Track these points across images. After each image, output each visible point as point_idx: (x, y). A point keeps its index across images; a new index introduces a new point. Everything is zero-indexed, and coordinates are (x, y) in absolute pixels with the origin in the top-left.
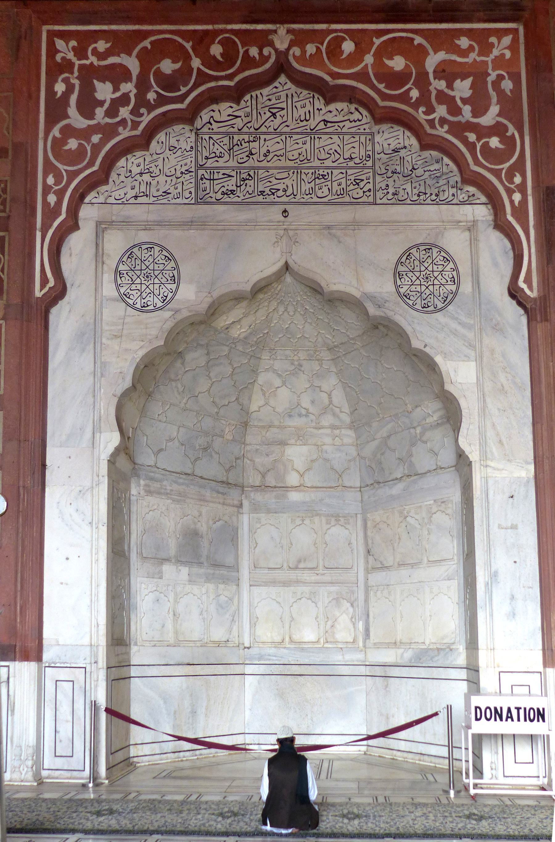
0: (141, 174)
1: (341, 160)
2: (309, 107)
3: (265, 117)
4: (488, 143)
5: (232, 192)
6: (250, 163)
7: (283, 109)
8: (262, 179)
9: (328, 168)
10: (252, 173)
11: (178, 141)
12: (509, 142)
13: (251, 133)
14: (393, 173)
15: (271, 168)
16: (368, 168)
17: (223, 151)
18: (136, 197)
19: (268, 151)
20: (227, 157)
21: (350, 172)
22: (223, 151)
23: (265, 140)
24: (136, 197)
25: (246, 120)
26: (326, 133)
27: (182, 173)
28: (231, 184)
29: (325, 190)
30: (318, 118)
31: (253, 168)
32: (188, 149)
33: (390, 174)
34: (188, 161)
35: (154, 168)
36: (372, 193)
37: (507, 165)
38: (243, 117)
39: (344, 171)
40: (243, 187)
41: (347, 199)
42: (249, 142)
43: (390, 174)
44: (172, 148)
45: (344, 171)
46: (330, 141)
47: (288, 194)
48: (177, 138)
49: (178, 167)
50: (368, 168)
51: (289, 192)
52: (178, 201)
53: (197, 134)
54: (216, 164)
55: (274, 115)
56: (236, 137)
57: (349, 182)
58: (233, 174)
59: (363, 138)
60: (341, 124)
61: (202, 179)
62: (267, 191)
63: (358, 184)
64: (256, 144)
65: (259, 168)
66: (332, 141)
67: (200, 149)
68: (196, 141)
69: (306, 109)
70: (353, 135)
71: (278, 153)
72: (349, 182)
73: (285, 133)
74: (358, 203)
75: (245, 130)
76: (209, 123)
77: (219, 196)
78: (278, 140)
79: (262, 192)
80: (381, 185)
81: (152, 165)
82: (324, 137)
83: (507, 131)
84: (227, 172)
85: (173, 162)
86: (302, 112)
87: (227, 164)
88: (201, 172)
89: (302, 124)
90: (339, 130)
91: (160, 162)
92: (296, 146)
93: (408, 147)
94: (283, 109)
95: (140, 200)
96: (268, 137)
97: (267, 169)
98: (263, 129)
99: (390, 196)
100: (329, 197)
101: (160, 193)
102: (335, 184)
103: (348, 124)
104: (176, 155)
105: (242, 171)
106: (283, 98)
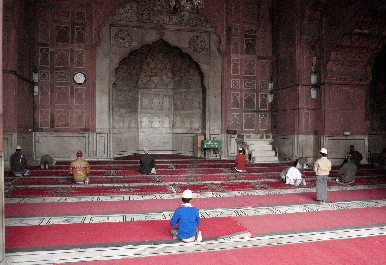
0: (122, 13)
5: (147, 20)
18: (121, 19)
23: (157, 7)
24: (121, 19)
28: (147, 17)
29: (172, 21)
32: (135, 7)
34: (135, 11)
44: (131, 7)
51: (162, 21)
53: (138, 4)
54: (143, 12)
56: (149, 6)
58: (148, 15)
64: (154, 8)
68: (138, 6)
77: (144, 20)
79: (155, 20)
84: (146, 14)
95: (122, 20)
96: (158, 6)
97: (157, 15)
98: (156, 4)
102: (175, 20)
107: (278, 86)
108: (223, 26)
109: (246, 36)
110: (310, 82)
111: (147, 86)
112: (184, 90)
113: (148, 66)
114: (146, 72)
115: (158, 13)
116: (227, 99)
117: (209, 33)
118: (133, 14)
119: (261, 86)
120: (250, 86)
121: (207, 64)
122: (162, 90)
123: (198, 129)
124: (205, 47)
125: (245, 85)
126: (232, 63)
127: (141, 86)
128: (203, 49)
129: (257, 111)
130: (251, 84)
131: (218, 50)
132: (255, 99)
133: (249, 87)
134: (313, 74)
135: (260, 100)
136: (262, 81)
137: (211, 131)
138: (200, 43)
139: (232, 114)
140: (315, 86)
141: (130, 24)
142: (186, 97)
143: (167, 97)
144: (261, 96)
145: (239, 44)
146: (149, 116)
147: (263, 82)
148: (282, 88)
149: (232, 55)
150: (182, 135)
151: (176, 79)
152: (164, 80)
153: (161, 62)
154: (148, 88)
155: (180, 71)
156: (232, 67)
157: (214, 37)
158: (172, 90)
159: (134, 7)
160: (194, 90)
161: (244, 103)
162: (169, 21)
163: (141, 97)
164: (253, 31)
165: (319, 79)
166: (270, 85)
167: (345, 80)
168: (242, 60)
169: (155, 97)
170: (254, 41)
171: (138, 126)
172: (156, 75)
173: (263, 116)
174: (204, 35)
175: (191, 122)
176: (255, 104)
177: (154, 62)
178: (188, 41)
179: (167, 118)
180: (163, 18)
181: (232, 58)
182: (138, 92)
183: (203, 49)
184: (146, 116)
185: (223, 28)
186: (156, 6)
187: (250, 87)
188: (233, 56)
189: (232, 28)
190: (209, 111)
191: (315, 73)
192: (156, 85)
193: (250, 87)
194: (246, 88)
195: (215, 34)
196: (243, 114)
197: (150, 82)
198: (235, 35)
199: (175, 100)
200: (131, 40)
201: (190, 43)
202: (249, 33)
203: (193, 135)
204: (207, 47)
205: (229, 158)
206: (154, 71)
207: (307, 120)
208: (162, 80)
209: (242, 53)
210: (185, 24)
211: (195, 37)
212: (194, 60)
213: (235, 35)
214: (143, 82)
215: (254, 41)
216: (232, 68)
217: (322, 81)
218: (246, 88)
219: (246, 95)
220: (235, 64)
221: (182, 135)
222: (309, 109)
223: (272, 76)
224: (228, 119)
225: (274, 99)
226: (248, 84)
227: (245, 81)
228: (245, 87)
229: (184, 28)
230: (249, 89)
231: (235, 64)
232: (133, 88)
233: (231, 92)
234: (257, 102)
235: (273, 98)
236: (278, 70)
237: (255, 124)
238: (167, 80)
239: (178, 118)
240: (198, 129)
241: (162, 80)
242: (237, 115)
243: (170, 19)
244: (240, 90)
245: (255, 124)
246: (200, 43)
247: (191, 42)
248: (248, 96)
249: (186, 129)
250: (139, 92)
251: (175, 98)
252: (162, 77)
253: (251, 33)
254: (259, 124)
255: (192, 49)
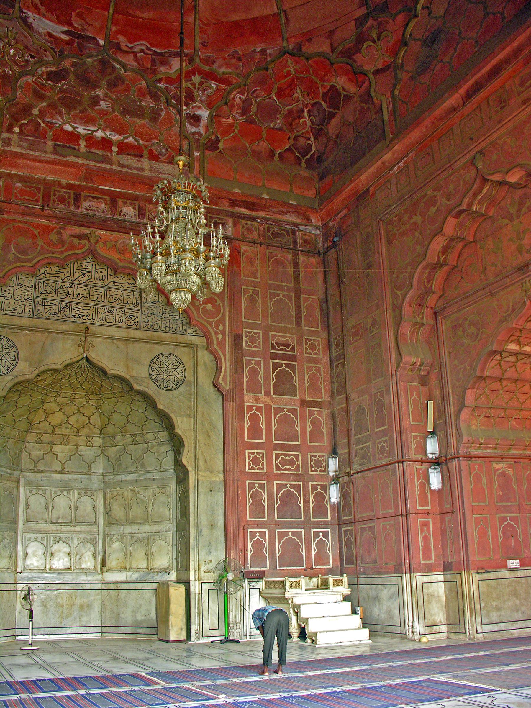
1: (122, 304)
2: (105, 273)
3: (78, 275)
4: (206, 307)
5: (56, 313)
6: (67, 299)
7: (90, 272)
8: (75, 309)
9: (115, 307)
10: (68, 305)
11: (24, 281)
12: (218, 308)
13: (69, 283)
14: (151, 314)
15: (80, 303)
16: (138, 310)
17: (51, 290)
19: (79, 294)
20: (53, 294)
21: (127, 311)
22: (51, 290)
23: (77, 287)
25: (67, 275)
26: (115, 289)
27: (25, 299)
28: (55, 309)
30: (110, 280)
31: (69, 302)
32: (30, 286)
33: (149, 315)
35: (7, 294)
36: (139, 324)
37: (215, 319)
38: (65, 273)
39: (123, 310)
40: (62, 312)
41: (124, 325)
42: (68, 287)
43: (149, 315)
44: (20, 285)
45: (123, 310)
46: (116, 293)
47: (89, 318)
48: (24, 279)
49: (23, 296)
50: (138, 310)
51: (90, 318)
52: (21, 315)
53: (36, 279)
54: (47, 297)
55: (84, 274)
56: (60, 284)
57: (126, 316)
58: (57, 303)
59: (135, 293)
60: (123, 285)
61: (37, 304)
62: (77, 315)
63: (131, 318)
64: (72, 289)
65: (73, 302)
66: (117, 293)
67: (37, 287)
68: (36, 282)
69: (103, 274)
70: (130, 291)
71: (85, 296)
72: (126, 316)
73: (91, 285)
74: (131, 328)
75: (66, 280)
76: (44, 273)
77: (47, 315)
78: (86, 288)
79: (74, 316)
80: (144, 320)
81: (7, 292)
82: (113, 290)
83: (216, 302)
84: (53, 302)
85: (21, 293)
86: (101, 275)
87: (53, 298)
88: (37, 300)
89: (100, 282)
90: (122, 288)
91: (12, 291)
92: (96, 293)
93: (161, 302)
94: (90, 272)
96: (79, 286)
97: (78, 304)
98: (76, 282)
99: (149, 327)
100: (114, 323)
101: (10, 309)
103: (126, 285)
104: (22, 289)
105: (63, 303)
106: (90, 266)
107: (350, 465)
108: (223, 333)
109: (274, 356)
110: (426, 453)
111: (41, 467)
112: (132, 477)
113: (46, 420)
114: (40, 433)
115: (79, 301)
116: (238, 498)
117: (192, 347)
118: (23, 300)
119: (312, 467)
120: (287, 467)
121: (189, 416)
122: (75, 476)
123: (167, 571)
124: (185, 379)
125: (277, 464)
126: (247, 414)
127: (27, 467)
128: (180, 383)
129: (307, 525)
130: (291, 463)
131: (215, 386)
132: (300, 495)
133: (286, 470)
134: (430, 436)
135: (311, 498)
136: (313, 456)
137: (202, 573)
138: (173, 370)
139: (251, 532)
140: (437, 462)
141: (17, 321)
142: (136, 494)
143: (89, 494)
144: (314, 488)
145: (261, 372)
146: (42, 539)
147: (315, 456)
148: (362, 469)
149: (246, 398)
150: (126, 586)
151: (112, 451)
152: (82, 453)
153: (79, 411)
154: (43, 471)
155: (122, 432)
156: (247, 423)
157: (204, 356)
158: (101, 477)
159: (27, 285)
160: (157, 476)
161: (276, 506)
162: (104, 319)
163: (25, 494)
164: (288, 346)
165: (443, 446)
166: (333, 465)
167: (495, 448)
168: (268, 408)
169: (59, 493)
170: (292, 367)
171: (16, 565)
172: (65, 440)
173: (321, 534)
174: (183, 354)
175: (149, 555)
176: (302, 506)
177: (60, 410)
178: (147, 363)
179: (89, 545)
180: (91, 313)
181: (246, 404)
182: (18, 481)
183: (179, 384)
184: (36, 540)
185: (224, 338)
186: (76, 286)
187: (289, 470)
188: (249, 400)
189: (244, 337)
190: (197, 525)
191: (433, 433)
192: (63, 465)
193: (289, 470)
194: (279, 472)
195: (207, 349)
196: (277, 531)
197: (48, 457)
198: (253, 354)
199: (108, 502)
200: (16, 358)
201: (151, 368)
202: (281, 350)
203: (155, 586)
204: (189, 377)
205: (248, 639)
206: (58, 431)
207: (426, 539)
208: (76, 452)
209: (267, 394)
210: (140, 326)
211: (163, 354)
212: (160, 407)
213: (253, 354)
214: (33, 457)
215: (292, 367)
216: (246, 427)
217: (452, 450)
218: (279, 472)
219: (280, 487)
220: (254, 418)
221: (126, 586)
222: (428, 514)
223: (335, 444)
224: (241, 545)
225: (344, 495)
226: (284, 462)
227: (277, 456)
228: (278, 468)
229: (137, 334)
230: (287, 472)
231: (254, 418)
232: (9, 471)
233: (248, 482)
234: (306, 502)
235: (341, 491)
236: (349, 430)
237: (304, 554)
238: (87, 453)
239: (116, 545)
240: (167, 571)
241: (76, 452)
242: (262, 534)
243: (108, 314)
244: (269, 476)
245: (304, 554)
246: (173, 370)
247: (153, 365)
248: (286, 490)
249: (137, 570)
250: (22, 482)
251: (108, 496)
252: (77, 446)
253: (285, 350)
254: (313, 554)
255: (154, 381)
